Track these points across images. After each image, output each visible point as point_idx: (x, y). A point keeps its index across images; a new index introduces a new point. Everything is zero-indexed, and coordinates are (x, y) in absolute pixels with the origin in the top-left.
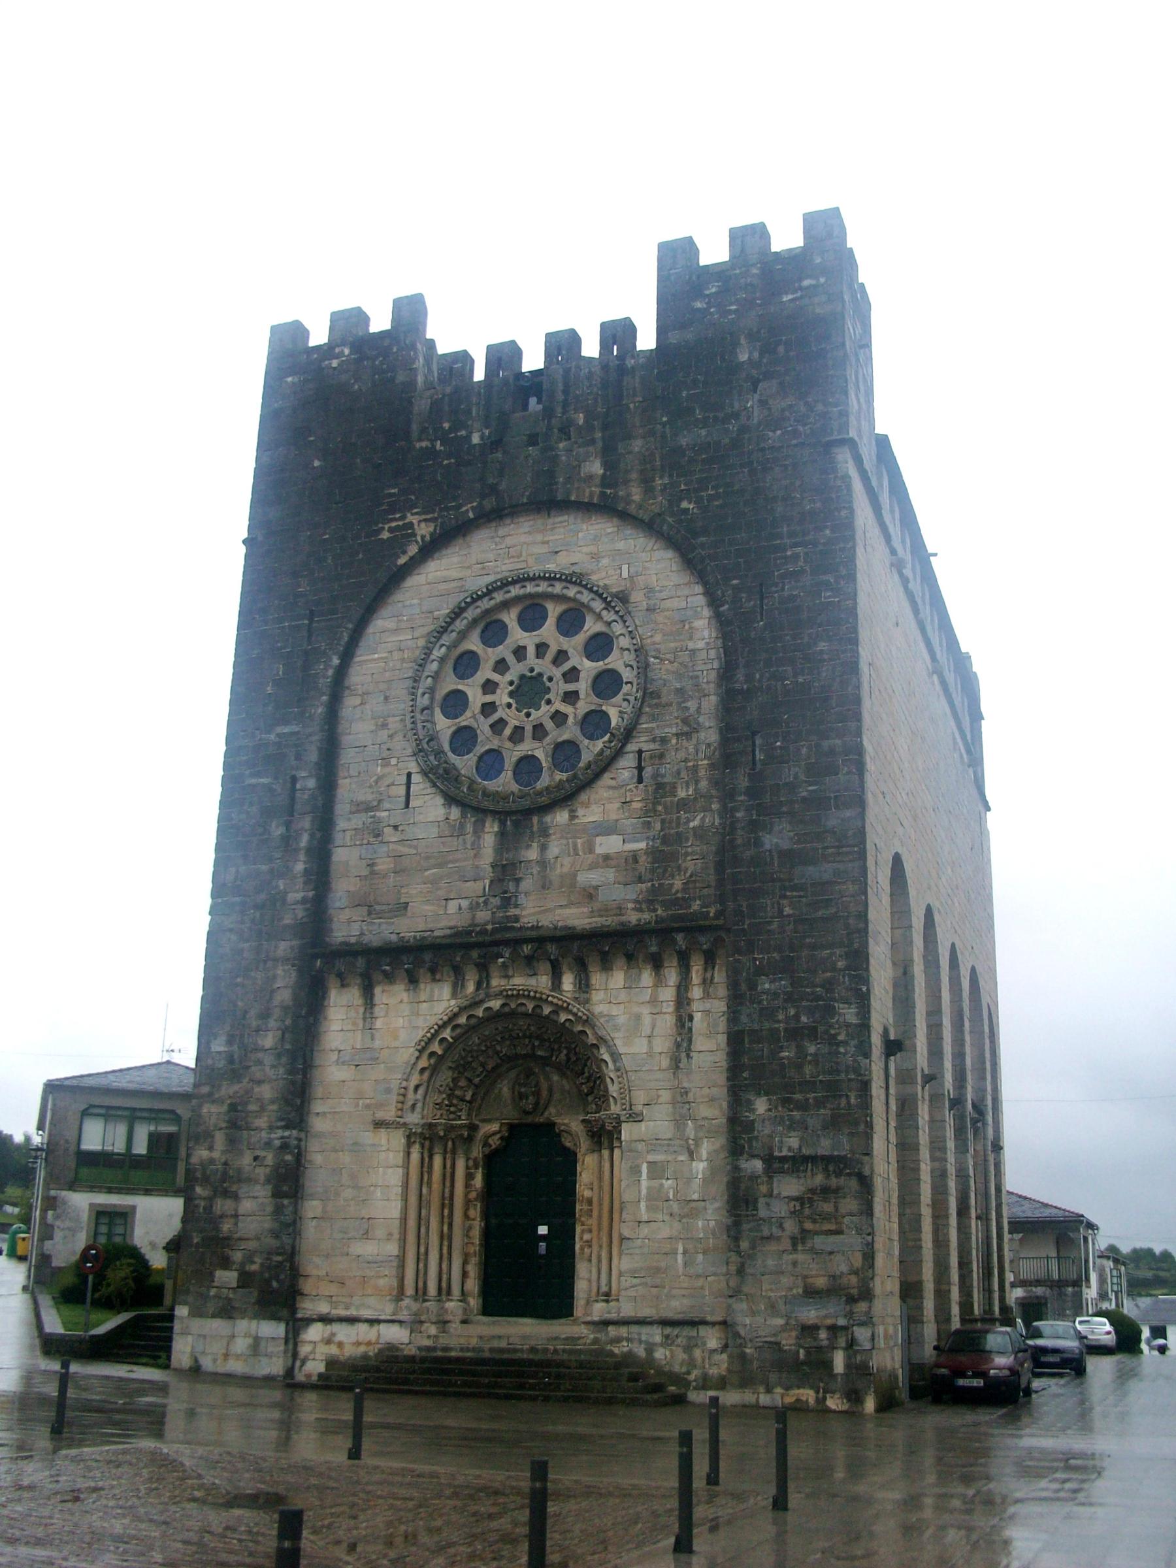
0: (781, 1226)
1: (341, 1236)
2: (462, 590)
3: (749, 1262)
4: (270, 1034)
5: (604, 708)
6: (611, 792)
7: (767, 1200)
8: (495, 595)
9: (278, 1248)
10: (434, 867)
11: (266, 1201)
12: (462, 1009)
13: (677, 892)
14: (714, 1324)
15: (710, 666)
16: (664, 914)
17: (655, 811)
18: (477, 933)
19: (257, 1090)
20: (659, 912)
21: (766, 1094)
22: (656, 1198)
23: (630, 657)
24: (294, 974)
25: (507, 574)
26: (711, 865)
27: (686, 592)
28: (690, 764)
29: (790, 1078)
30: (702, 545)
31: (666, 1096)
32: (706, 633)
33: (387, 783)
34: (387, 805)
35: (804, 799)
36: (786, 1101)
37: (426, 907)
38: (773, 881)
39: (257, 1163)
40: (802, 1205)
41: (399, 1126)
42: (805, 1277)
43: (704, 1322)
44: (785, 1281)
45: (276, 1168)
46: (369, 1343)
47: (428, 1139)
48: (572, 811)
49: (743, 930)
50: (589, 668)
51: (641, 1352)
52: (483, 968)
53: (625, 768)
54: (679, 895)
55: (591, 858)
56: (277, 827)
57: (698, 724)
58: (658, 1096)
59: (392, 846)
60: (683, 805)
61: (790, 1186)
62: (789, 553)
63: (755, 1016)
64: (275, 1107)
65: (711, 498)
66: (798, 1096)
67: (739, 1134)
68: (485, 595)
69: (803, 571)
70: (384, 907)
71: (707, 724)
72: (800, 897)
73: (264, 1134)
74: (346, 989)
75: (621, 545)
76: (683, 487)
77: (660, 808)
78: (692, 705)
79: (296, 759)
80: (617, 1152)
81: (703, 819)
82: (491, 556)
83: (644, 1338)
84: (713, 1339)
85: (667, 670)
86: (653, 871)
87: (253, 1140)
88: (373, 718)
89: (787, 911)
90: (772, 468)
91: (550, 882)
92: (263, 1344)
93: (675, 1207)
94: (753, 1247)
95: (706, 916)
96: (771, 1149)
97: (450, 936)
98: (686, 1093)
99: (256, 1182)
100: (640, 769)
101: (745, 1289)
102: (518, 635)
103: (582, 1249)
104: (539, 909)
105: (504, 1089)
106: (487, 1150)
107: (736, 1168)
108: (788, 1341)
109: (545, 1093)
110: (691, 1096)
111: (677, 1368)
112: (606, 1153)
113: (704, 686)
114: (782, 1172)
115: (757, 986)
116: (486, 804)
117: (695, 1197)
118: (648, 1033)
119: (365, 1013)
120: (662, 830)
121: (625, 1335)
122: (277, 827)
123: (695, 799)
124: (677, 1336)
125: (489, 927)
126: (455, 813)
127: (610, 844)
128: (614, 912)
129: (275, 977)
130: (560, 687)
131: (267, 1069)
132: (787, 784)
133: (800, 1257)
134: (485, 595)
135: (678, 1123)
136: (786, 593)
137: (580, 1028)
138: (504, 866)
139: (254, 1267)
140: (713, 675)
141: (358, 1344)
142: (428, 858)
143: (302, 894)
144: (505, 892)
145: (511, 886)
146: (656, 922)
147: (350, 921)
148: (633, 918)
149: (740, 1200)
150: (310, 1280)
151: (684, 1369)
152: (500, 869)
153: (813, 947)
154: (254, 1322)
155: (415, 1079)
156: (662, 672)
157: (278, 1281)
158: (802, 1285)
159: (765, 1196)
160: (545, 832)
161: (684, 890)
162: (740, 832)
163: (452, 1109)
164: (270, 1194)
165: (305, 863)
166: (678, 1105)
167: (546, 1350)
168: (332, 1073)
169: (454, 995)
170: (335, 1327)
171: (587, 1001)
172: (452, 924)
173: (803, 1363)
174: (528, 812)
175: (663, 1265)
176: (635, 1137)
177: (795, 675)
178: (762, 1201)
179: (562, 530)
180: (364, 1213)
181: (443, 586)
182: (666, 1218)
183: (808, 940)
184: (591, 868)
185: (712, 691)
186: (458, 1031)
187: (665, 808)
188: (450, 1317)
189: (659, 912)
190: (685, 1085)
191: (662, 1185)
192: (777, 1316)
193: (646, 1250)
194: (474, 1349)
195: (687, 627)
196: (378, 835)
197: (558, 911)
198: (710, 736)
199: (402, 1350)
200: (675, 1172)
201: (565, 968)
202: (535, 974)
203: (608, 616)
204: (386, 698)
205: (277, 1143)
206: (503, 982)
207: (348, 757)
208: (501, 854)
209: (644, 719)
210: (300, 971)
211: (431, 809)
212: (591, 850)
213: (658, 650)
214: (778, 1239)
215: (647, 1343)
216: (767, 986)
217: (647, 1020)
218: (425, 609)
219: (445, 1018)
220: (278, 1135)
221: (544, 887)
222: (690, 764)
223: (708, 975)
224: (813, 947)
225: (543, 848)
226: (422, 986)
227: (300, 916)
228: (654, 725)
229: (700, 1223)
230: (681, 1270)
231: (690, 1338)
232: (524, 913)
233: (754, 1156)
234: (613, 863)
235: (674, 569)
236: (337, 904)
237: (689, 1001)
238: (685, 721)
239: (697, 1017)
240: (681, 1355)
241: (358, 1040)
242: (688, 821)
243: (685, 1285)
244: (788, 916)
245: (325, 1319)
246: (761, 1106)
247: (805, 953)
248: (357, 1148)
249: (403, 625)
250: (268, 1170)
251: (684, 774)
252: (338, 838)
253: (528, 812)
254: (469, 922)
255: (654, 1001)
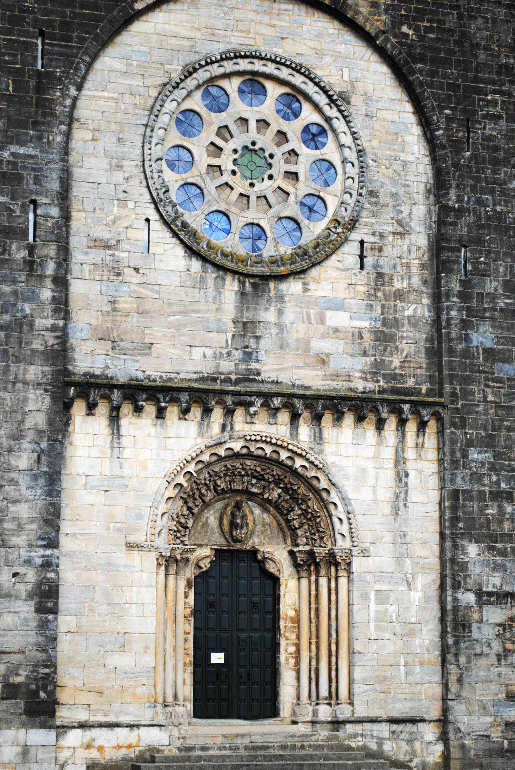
0: (489, 645)
1: (97, 649)
2: (192, 49)
3: (466, 673)
4: (25, 456)
5: (322, 194)
6: (338, 273)
7: (479, 625)
8: (225, 63)
9: (44, 661)
10: (179, 313)
11: (30, 616)
12: (207, 447)
13: (396, 368)
14: (431, 721)
15: (419, 179)
16: (385, 386)
17: (376, 297)
18: (222, 381)
19: (12, 508)
20: (381, 383)
21: (476, 542)
22: (382, 620)
23: (352, 155)
24: (48, 400)
25: (241, 48)
26: (423, 351)
27: (398, 107)
28: (405, 261)
29: (493, 530)
30: (421, 71)
31: (388, 537)
32: (416, 149)
33: (125, 225)
34: (124, 246)
35: (502, 310)
36: (491, 548)
37: (173, 351)
38: (480, 372)
39: (17, 579)
40: (504, 630)
41: (153, 548)
42: (507, 685)
43: (423, 720)
44: (494, 688)
45: (39, 585)
46: (130, 746)
47: (170, 562)
48: (304, 284)
49: (457, 409)
50: (307, 154)
51: (373, 745)
52: (229, 412)
53: (349, 252)
54: (398, 371)
55: (322, 329)
56: (19, 249)
57: (411, 228)
58: (383, 537)
59: (133, 287)
60: (399, 295)
61: (495, 615)
62: (489, 97)
63: (467, 479)
64: (34, 526)
65: (429, 30)
66: (499, 545)
67: (451, 573)
68: (217, 61)
69: (499, 117)
70: (127, 345)
71: (418, 229)
72: (501, 388)
73: (23, 552)
74: (91, 418)
75: (342, 48)
76: (403, 12)
77: (380, 294)
78: (405, 209)
79: (35, 184)
80: (343, 581)
81: (415, 309)
82: (220, 24)
83: (375, 734)
84: (429, 732)
85: (384, 174)
86: (375, 347)
87: (10, 557)
88: (106, 156)
89: (490, 398)
90: (476, 18)
91: (287, 344)
92: (33, 751)
93: (398, 628)
94: (469, 662)
95: (419, 393)
96: (480, 584)
97: (196, 380)
98: (405, 535)
99: (17, 597)
100: (362, 257)
101: (464, 694)
102: (239, 107)
103: (287, 660)
104: (277, 367)
105: (211, 517)
106: (198, 572)
107: (455, 599)
108: (496, 734)
109: (251, 524)
110: (408, 539)
111: (402, 758)
112: (323, 581)
113: (415, 195)
114: (489, 603)
115: (468, 455)
116: (229, 264)
117: (413, 620)
118: (373, 484)
119: (112, 441)
120: (382, 314)
121: (360, 732)
122: (19, 249)
123: (409, 291)
124: (401, 732)
125: (233, 377)
126: (196, 265)
127: (338, 319)
128: (343, 379)
129: (26, 400)
130: (280, 166)
131: (23, 489)
132: (489, 294)
133: (503, 669)
134: (217, 61)
135: (399, 559)
136: (487, 132)
137: (313, 474)
138: (245, 324)
139: (19, 680)
140: (422, 188)
141: (119, 747)
142: (170, 304)
143: (52, 322)
144: (247, 347)
145: (252, 343)
146: (379, 392)
147: (93, 353)
148: (360, 385)
149: (454, 626)
150: (66, 690)
151: (407, 758)
152: (241, 325)
153: (509, 429)
154: (22, 732)
155: (163, 507)
156: (380, 176)
157: (45, 692)
158: (505, 691)
159: (477, 622)
160: (281, 298)
161: (401, 367)
162: (453, 328)
163: (179, 535)
164: (33, 609)
165: (53, 291)
166: (398, 545)
167: (294, 747)
168: (79, 496)
169: (201, 434)
170: (96, 732)
171: (321, 452)
172: (199, 369)
173: (507, 751)
174: (266, 278)
175: (389, 674)
176: (364, 570)
177: (494, 205)
178: (474, 626)
179: (287, 18)
180: (120, 628)
181: (172, 41)
182: (391, 636)
183: (505, 423)
184: (323, 336)
185: (421, 201)
186: (200, 466)
187: (385, 295)
188: (182, 721)
189: (381, 383)
190: (404, 529)
191: (386, 610)
192: (488, 715)
193: (375, 662)
194: (230, 748)
195: (400, 139)
196: (119, 274)
197: (295, 371)
198: (420, 239)
199: (163, 751)
200: (397, 599)
201: (301, 421)
202: (276, 424)
203: (332, 112)
204: (119, 140)
205: (39, 561)
206: (247, 427)
207: (79, 191)
208: (242, 312)
209: (364, 213)
210: (54, 398)
211: (171, 256)
212: (322, 322)
213: (375, 154)
214: (487, 655)
215: (378, 738)
216: (475, 456)
217: (372, 472)
218: (155, 59)
219: (194, 455)
220: (38, 554)
221: (281, 347)
222: (405, 261)
223: (420, 440)
224: (509, 429)
225: (280, 312)
226: (168, 422)
227: (50, 343)
228: (373, 220)
229: (417, 641)
230: (403, 678)
231: (411, 733)
232: (264, 368)
233: (468, 590)
234: (342, 335)
235: (388, 84)
236: (79, 335)
237: (405, 461)
238: (400, 223)
239: (412, 474)
240: (405, 747)
241: (107, 467)
242: (404, 309)
243: (407, 691)
244: (491, 402)
245: (83, 726)
246: (473, 550)
247: (503, 433)
248: (109, 566)
249: (134, 70)
250: (30, 586)
251: (399, 268)
252: (75, 270)
253: (266, 278)
254: (214, 370)
255: (376, 457)
